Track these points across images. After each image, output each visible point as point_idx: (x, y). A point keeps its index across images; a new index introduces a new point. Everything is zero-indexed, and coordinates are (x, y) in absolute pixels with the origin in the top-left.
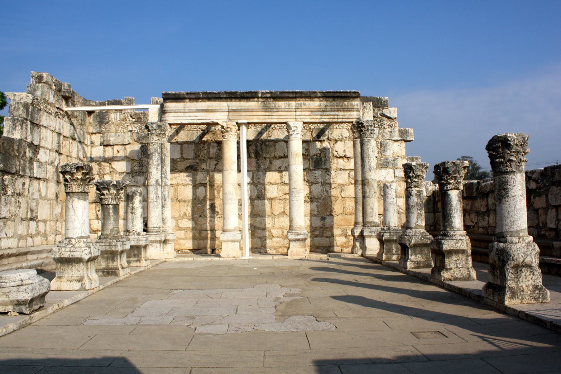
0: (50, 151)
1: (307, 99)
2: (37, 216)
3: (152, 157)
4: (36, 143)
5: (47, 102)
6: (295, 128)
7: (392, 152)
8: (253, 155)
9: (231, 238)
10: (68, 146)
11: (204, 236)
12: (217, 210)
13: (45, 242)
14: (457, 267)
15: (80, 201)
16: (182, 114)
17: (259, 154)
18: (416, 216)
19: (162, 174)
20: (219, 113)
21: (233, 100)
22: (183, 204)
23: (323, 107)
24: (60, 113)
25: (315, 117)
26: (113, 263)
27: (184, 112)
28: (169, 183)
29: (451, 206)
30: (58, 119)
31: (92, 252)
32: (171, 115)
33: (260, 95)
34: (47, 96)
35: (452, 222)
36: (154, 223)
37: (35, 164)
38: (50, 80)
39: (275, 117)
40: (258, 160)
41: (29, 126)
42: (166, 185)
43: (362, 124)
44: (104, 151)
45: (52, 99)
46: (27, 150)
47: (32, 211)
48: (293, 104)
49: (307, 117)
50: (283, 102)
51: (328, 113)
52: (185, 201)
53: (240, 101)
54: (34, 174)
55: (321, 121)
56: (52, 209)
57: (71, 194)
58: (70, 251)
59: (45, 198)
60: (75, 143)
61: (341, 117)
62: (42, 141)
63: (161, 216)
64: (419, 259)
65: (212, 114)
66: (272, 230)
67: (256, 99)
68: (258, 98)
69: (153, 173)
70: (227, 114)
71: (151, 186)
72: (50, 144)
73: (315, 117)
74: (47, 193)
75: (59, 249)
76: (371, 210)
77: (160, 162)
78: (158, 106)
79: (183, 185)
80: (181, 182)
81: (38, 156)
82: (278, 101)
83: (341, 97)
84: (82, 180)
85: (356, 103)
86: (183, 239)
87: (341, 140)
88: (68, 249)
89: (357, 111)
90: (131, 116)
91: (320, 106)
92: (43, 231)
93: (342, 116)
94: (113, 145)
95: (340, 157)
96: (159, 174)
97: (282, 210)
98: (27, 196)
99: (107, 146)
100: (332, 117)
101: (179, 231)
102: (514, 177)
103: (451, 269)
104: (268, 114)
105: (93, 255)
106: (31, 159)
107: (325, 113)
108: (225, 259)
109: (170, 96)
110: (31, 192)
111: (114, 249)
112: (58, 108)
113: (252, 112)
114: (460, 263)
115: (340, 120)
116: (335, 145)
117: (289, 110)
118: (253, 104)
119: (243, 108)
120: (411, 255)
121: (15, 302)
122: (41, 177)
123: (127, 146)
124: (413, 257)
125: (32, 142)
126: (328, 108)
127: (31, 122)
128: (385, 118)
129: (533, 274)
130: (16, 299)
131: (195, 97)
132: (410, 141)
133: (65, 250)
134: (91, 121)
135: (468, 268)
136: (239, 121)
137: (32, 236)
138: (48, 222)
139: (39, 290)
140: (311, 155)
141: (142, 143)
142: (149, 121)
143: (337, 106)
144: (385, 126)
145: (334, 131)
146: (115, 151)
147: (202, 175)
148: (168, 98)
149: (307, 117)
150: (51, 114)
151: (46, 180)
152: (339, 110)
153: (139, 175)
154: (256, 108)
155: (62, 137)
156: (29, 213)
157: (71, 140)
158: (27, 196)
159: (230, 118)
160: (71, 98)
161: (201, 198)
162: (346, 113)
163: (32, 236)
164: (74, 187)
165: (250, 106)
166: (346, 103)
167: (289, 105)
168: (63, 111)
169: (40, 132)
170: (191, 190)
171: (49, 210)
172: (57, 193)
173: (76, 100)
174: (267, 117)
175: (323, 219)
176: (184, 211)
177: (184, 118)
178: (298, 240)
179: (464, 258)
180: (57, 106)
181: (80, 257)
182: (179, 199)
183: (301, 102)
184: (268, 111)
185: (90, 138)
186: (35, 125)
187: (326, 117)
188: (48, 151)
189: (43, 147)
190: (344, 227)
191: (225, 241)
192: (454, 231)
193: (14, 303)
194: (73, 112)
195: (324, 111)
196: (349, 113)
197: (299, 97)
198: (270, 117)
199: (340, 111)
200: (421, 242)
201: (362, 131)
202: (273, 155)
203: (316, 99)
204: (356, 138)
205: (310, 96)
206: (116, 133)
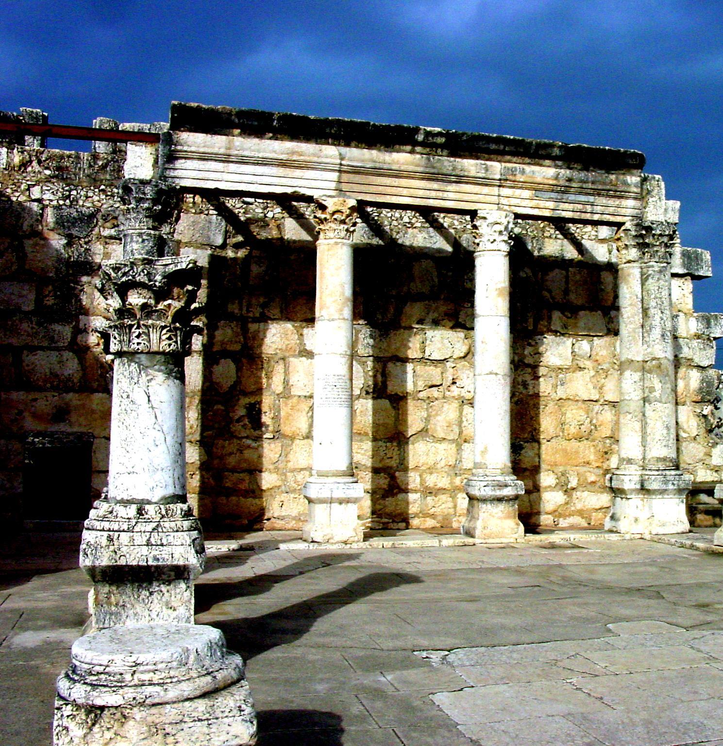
1: (527, 160)
9: (339, 494)
15: (170, 382)
20: (318, 172)
23: (562, 182)
25: (542, 204)
33: (420, 138)
39: (451, 196)
43: (649, 229)
48: (496, 168)
51: (572, 197)
55: (558, 214)
57: (143, 358)
58: (148, 544)
61: (598, 209)
65: (298, 173)
66: (397, 474)
67: (409, 148)
70: (335, 176)
73: (542, 204)
75: (110, 539)
76: (665, 432)
82: (460, 157)
85: (633, 179)
88: (141, 539)
89: (635, 199)
91: (556, 178)
93: (603, 208)
97: (422, 425)
100: (580, 207)
104: (435, 185)
107: (565, 196)
108: (323, 547)
113: (397, 177)
115: (596, 217)
117: (485, 182)
118: (402, 158)
126: (574, 185)
132: (700, 278)
133: (132, 539)
143: (593, 183)
145: (546, 244)
147: (229, 331)
159: (344, 187)
162: (611, 202)
164: (154, 336)
165: (393, 162)
166: (613, 177)
167: (487, 169)
178: (500, 500)
181: (181, 563)
184: (437, 180)
190: (561, 469)
191: (322, 501)
195: (563, 192)
196: (617, 202)
198: (440, 194)
199: (599, 195)
201: (647, 245)
203: (547, 162)
204: (629, 262)
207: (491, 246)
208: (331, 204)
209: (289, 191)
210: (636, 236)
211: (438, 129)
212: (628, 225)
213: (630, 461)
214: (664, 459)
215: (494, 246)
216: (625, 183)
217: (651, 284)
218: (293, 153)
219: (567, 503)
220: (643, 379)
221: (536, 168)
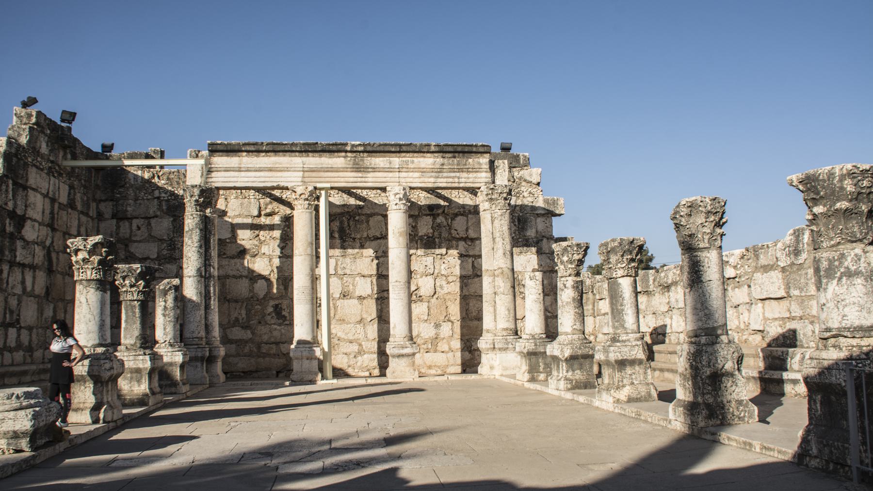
0: (40, 224)
2: (18, 321)
3: (191, 235)
4: (19, 212)
5: (36, 152)
6: (398, 196)
7: (534, 230)
8: (337, 235)
10: (65, 219)
11: (264, 351)
12: (284, 313)
13: (29, 360)
14: (632, 383)
16: (236, 174)
17: (344, 231)
18: (573, 317)
19: (205, 261)
21: (310, 154)
22: (234, 305)
23: (438, 166)
24: (54, 171)
25: (426, 180)
26: (139, 386)
27: (239, 170)
28: (216, 274)
29: (623, 299)
30: (52, 178)
31: (115, 366)
32: (219, 174)
34: (38, 144)
35: (624, 321)
36: (193, 332)
37: (19, 244)
38: (42, 121)
39: (370, 180)
40: (344, 241)
41: (11, 186)
42: (210, 276)
44: (118, 227)
45: (44, 148)
46: (8, 221)
47: (12, 312)
48: (396, 161)
49: (416, 180)
50: (381, 159)
51: (445, 175)
52: (236, 301)
53: (320, 156)
54: (16, 257)
56: (41, 311)
59: (32, 295)
60: (75, 214)
61: (463, 180)
62: (29, 209)
63: (203, 322)
64: (577, 377)
65: (279, 174)
68: (346, 152)
69: (192, 258)
71: (190, 277)
72: (40, 214)
73: (426, 180)
74: (33, 286)
76: (507, 312)
77: (203, 242)
78: (202, 162)
79: (234, 277)
80: (231, 273)
81: (24, 232)
83: (464, 152)
84: (100, 262)
86: (233, 356)
87: (462, 215)
90: (159, 177)
92: (27, 343)
94: (132, 219)
95: (462, 239)
96: (201, 260)
98: (5, 291)
99: (122, 219)
100: (451, 180)
101: (228, 345)
102: (708, 255)
103: (624, 386)
104: (360, 175)
105: (115, 372)
106: (12, 234)
107: (441, 174)
109: (219, 147)
110: (10, 285)
111: (141, 366)
112: (52, 162)
114: (636, 378)
115: (461, 185)
116: (454, 222)
117: (390, 170)
118: (338, 161)
119: (324, 166)
120: (567, 372)
121: (11, 433)
122: (27, 262)
123: (153, 221)
124: (570, 373)
125: (14, 211)
127: (13, 181)
128: (524, 183)
129: (737, 386)
130: (12, 429)
131: (256, 149)
132: (560, 215)
134: (99, 182)
135: (648, 384)
136: (319, 185)
137: (11, 350)
138: (35, 330)
139: (46, 416)
140: (420, 234)
141: (174, 216)
142: (189, 183)
143: (458, 165)
144: (526, 194)
146: (134, 227)
148: (214, 149)
149: (416, 180)
150: (42, 170)
151: (33, 267)
152: (461, 170)
153: (168, 263)
154: (344, 166)
155: (56, 206)
156: (8, 316)
157: (70, 210)
158: (5, 291)
159: (306, 180)
160: (70, 147)
161: (261, 296)
162: (471, 175)
163: (11, 350)
166: (470, 160)
167: (390, 163)
168: (59, 166)
169: (26, 196)
170: (247, 285)
171: (36, 313)
172: (47, 288)
173: (78, 151)
174: (359, 180)
175: (437, 326)
176: (236, 315)
177: (240, 179)
179: (642, 371)
180: (51, 158)
182: (228, 297)
183: (407, 158)
185: (97, 208)
186: (22, 186)
187: (442, 180)
188: (37, 225)
189: (31, 219)
192: (627, 333)
193: (9, 436)
194: (73, 168)
196: (475, 175)
197: (404, 152)
198: (363, 179)
200: (580, 352)
202: (365, 235)
203: (429, 155)
205: (422, 150)
206: (136, 200)
207: (395, 207)
208: (299, 190)
209: (275, 184)
210: (487, 195)
211: (358, 143)
212: (482, 189)
213: (488, 331)
214: (507, 329)
215: (397, 207)
216: (479, 163)
217: (497, 223)
218: (276, 163)
219: (472, 359)
220: (494, 281)
221: (422, 159)
